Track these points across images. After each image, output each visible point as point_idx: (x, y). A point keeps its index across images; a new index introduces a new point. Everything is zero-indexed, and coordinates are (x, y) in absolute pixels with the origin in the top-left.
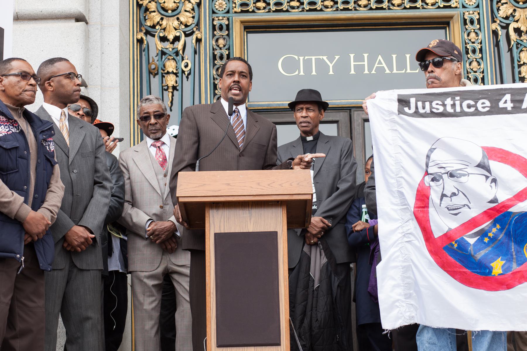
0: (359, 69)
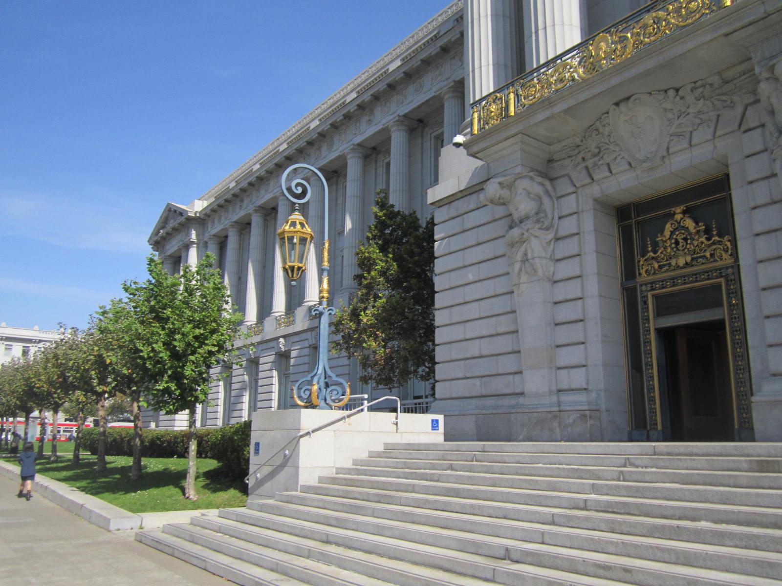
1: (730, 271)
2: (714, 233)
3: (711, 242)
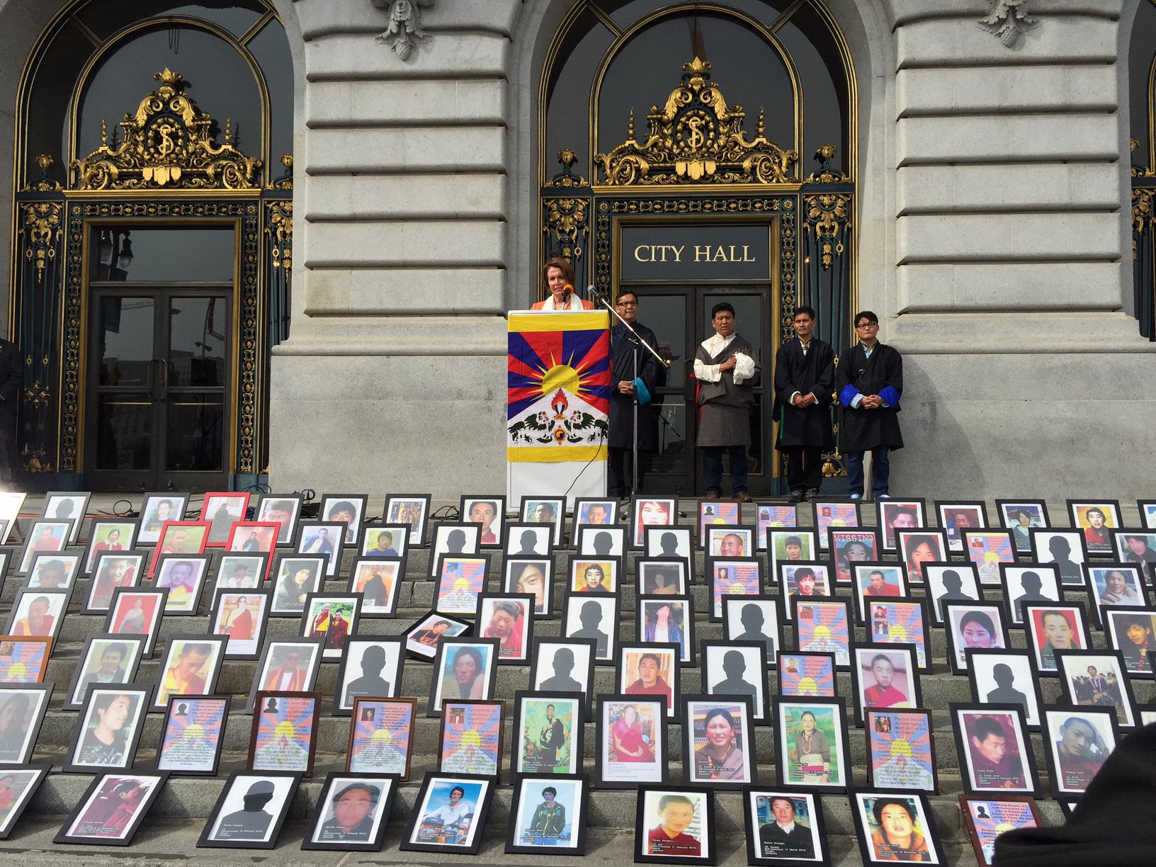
0: (703, 257)
1: (788, 204)
2: (761, 130)
3: (754, 144)
